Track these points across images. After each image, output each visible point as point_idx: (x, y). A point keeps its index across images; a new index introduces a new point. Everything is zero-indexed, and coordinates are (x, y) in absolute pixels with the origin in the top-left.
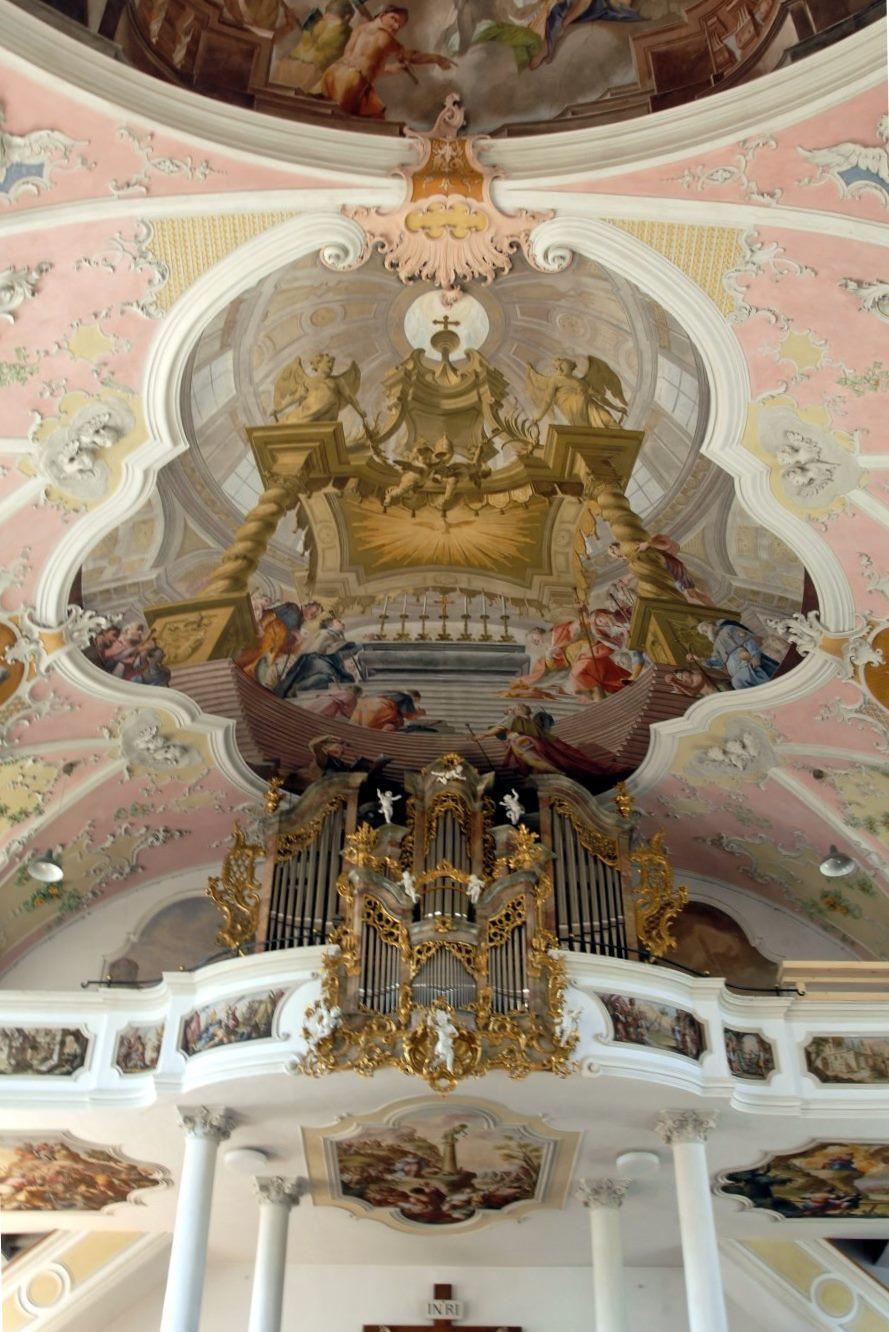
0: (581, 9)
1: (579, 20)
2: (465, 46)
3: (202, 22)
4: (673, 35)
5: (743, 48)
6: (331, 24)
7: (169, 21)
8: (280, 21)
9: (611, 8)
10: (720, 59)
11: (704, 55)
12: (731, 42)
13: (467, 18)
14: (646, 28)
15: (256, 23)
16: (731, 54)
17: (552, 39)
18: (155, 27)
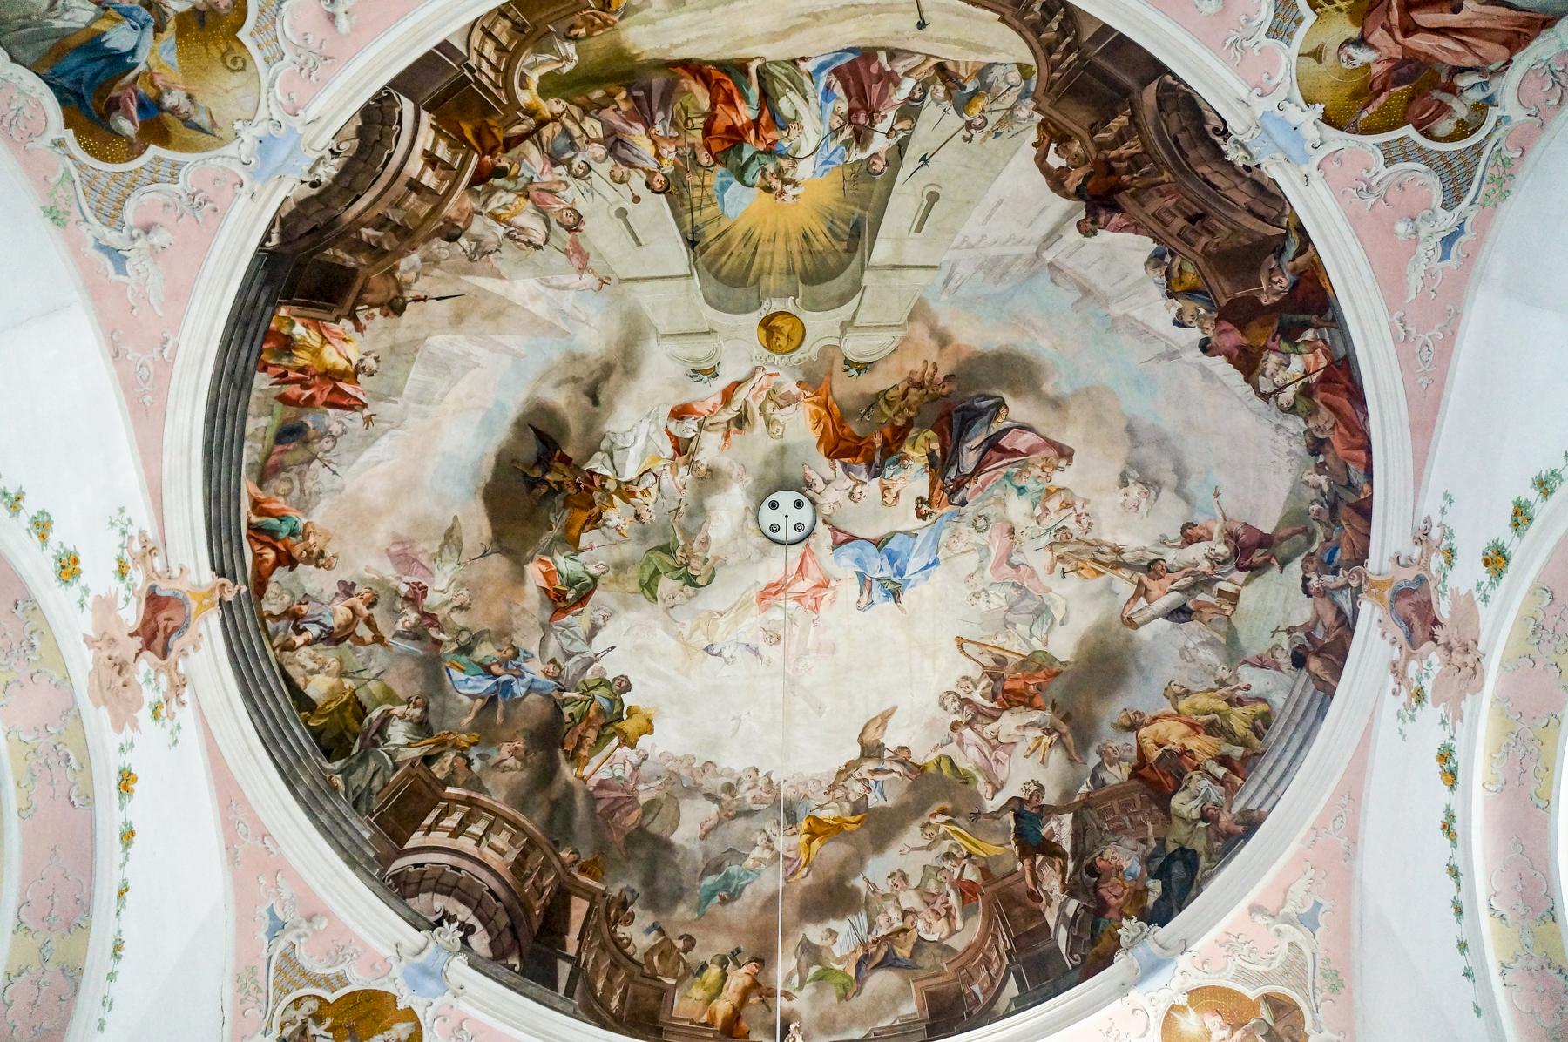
0: (878, 959)
1: (879, 966)
2: (801, 987)
3: (630, 977)
4: (940, 980)
5: (985, 993)
6: (714, 972)
7: (609, 979)
8: (681, 971)
9: (897, 959)
10: (970, 1000)
11: (959, 996)
12: (976, 988)
13: (803, 965)
14: (922, 974)
15: (664, 974)
16: (976, 996)
17: (860, 979)
18: (600, 985)
